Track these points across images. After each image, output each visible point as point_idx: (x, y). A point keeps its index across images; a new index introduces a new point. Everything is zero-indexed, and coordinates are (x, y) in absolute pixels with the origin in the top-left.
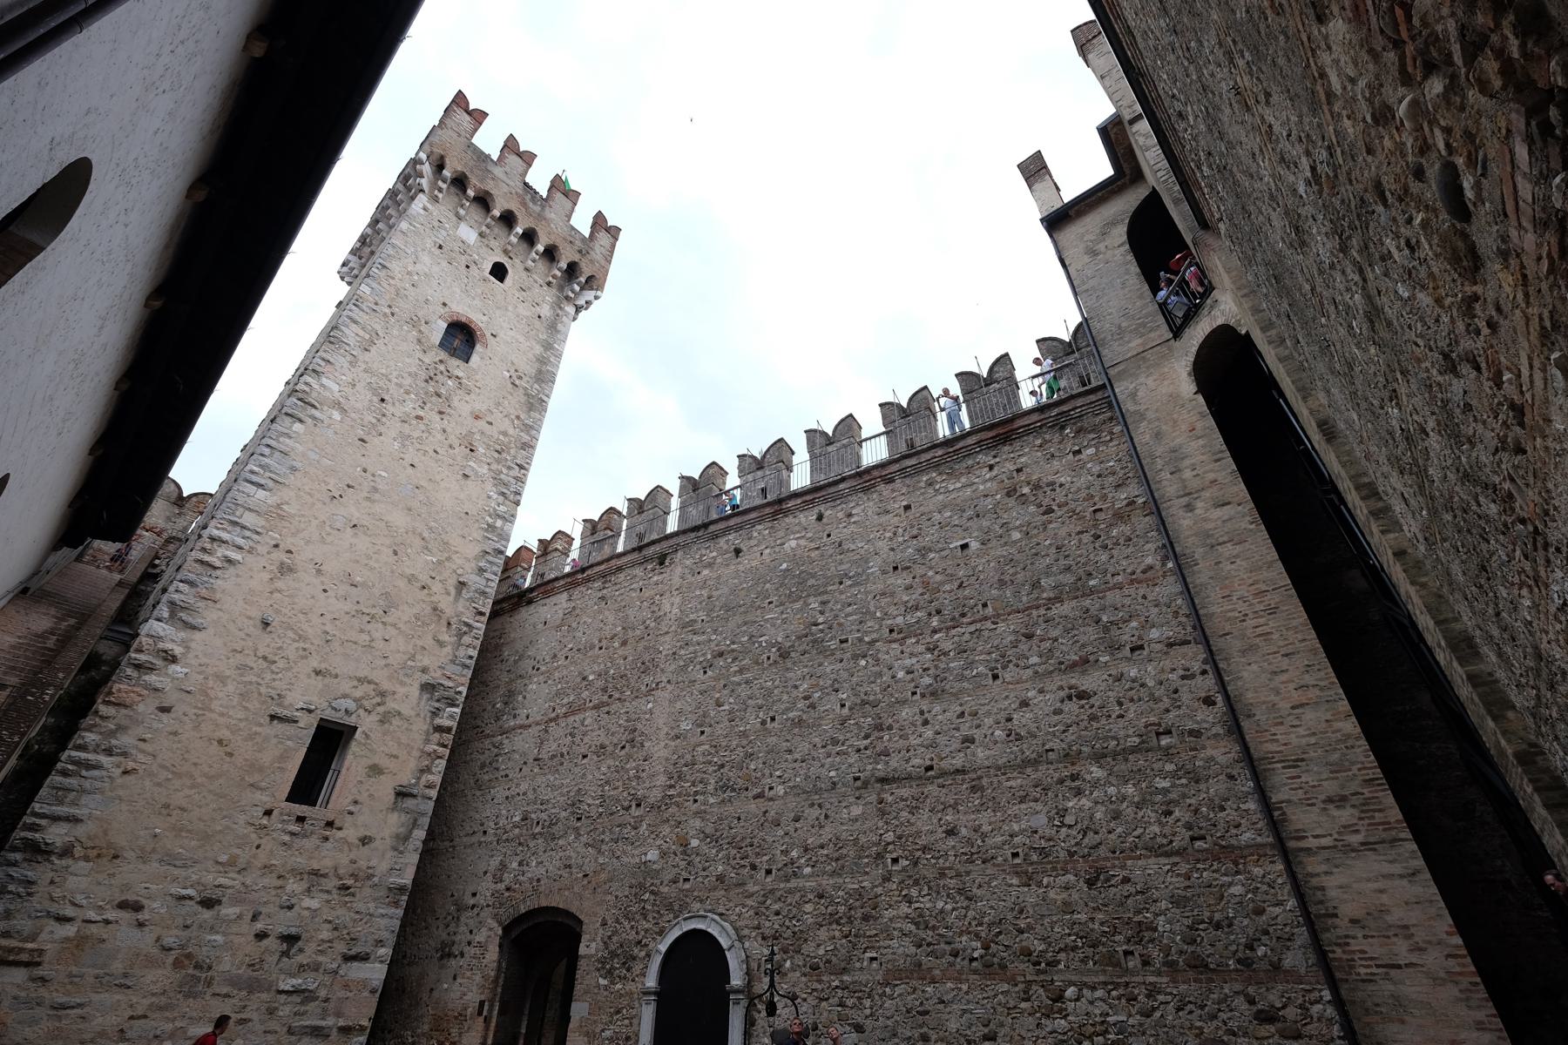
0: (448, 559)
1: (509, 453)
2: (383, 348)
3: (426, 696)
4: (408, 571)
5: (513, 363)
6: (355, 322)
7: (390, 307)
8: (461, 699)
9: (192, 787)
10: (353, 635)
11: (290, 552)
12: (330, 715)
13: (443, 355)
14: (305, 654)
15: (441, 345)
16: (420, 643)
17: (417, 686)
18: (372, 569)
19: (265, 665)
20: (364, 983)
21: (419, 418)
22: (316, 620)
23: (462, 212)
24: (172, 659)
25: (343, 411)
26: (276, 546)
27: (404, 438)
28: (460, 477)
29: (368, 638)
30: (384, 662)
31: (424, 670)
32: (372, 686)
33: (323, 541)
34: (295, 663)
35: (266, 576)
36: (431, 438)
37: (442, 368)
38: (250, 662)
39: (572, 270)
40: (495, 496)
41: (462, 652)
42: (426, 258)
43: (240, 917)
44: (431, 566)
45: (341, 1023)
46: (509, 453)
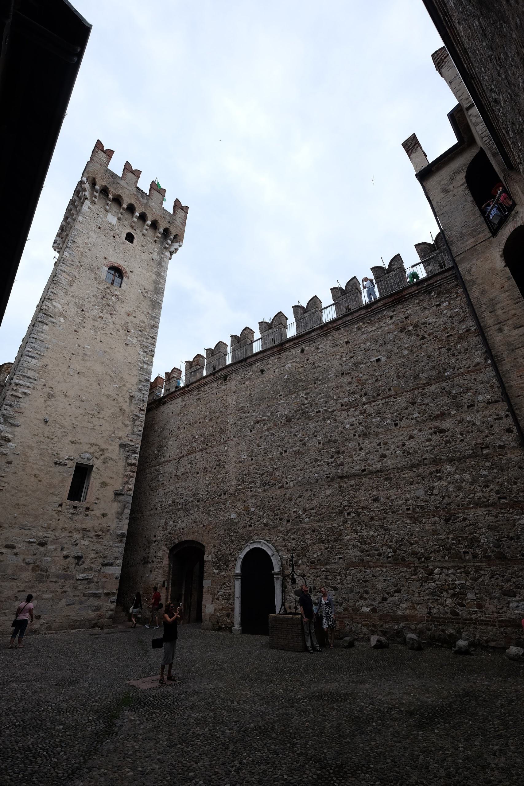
0: (124, 385)
1: (146, 331)
2: (79, 284)
3: (122, 450)
4: (106, 393)
5: (142, 285)
6: (64, 272)
7: (79, 262)
8: (138, 450)
9: (27, 495)
11: (51, 388)
12: (80, 461)
14: (65, 434)
16: (116, 426)
17: (117, 445)
18: (89, 393)
19: (49, 440)
20: (112, 575)
22: (68, 419)
23: (108, 207)
24: (9, 441)
25: (65, 318)
26: (45, 385)
27: (95, 328)
28: (124, 345)
29: (92, 425)
30: (101, 436)
31: (120, 438)
32: (97, 447)
33: (65, 381)
34: (62, 439)
35: (42, 400)
37: (109, 291)
38: (42, 439)
39: (166, 233)
40: (142, 353)
41: (136, 429)
42: (93, 235)
43: (56, 549)
45: (105, 591)
46: (146, 331)
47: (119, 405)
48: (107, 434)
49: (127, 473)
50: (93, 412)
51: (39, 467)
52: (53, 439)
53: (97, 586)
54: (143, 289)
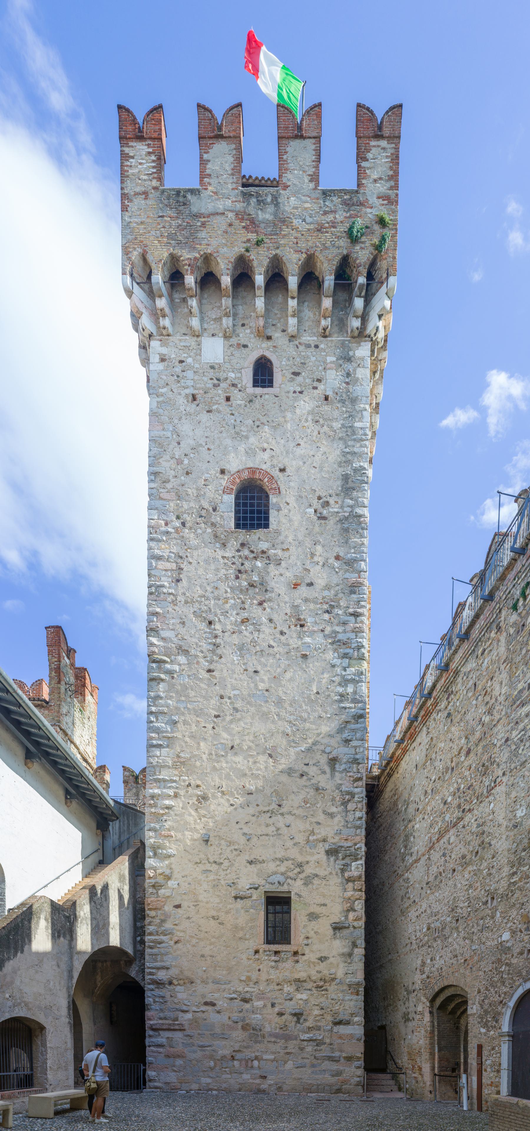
1: (339, 607)
3: (332, 859)
9: (211, 944)
10: (265, 830)
12: (269, 888)
13: (242, 535)
16: (314, 820)
17: (323, 852)
20: (352, 1036)
25: (186, 652)
28: (300, 659)
29: (274, 829)
31: (324, 840)
32: (290, 862)
37: (246, 552)
38: (208, 867)
40: (337, 662)
41: (350, 818)
42: (186, 427)
43: (265, 1006)
44: (302, 755)
45: (344, 1055)
47: (313, 781)
48: (300, 838)
49: (349, 894)
50: (271, 808)
51: (216, 905)
52: (222, 863)
53: (332, 1049)
54: (315, 502)
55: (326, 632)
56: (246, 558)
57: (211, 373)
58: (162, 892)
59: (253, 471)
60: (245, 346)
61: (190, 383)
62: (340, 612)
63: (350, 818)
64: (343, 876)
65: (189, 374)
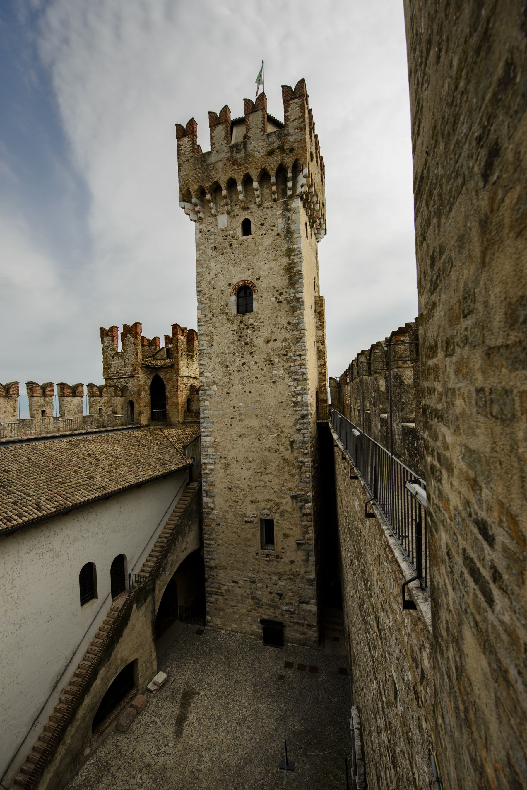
0: (282, 432)
4: (268, 446)
5: (274, 288)
6: (203, 335)
7: (211, 312)
8: (311, 499)
9: (234, 548)
10: (258, 483)
11: (225, 458)
12: (262, 517)
13: (240, 317)
14: (246, 496)
15: (239, 312)
16: (284, 478)
17: (289, 497)
18: (253, 452)
20: (310, 611)
21: (244, 364)
22: (244, 481)
23: (213, 212)
24: (213, 509)
25: (216, 384)
30: (272, 491)
31: (290, 489)
33: (233, 448)
35: (223, 470)
36: (252, 372)
37: (242, 326)
40: (291, 383)
42: (212, 265)
43: (263, 587)
44: (276, 439)
45: (306, 623)
46: (291, 351)
48: (277, 488)
50: (261, 470)
53: (299, 618)
55: (285, 367)
56: (243, 329)
57: (222, 234)
58: (211, 516)
59: (244, 282)
60: (237, 215)
61: (213, 241)
62: (292, 355)
63: (303, 477)
64: (301, 511)
65: (213, 236)
